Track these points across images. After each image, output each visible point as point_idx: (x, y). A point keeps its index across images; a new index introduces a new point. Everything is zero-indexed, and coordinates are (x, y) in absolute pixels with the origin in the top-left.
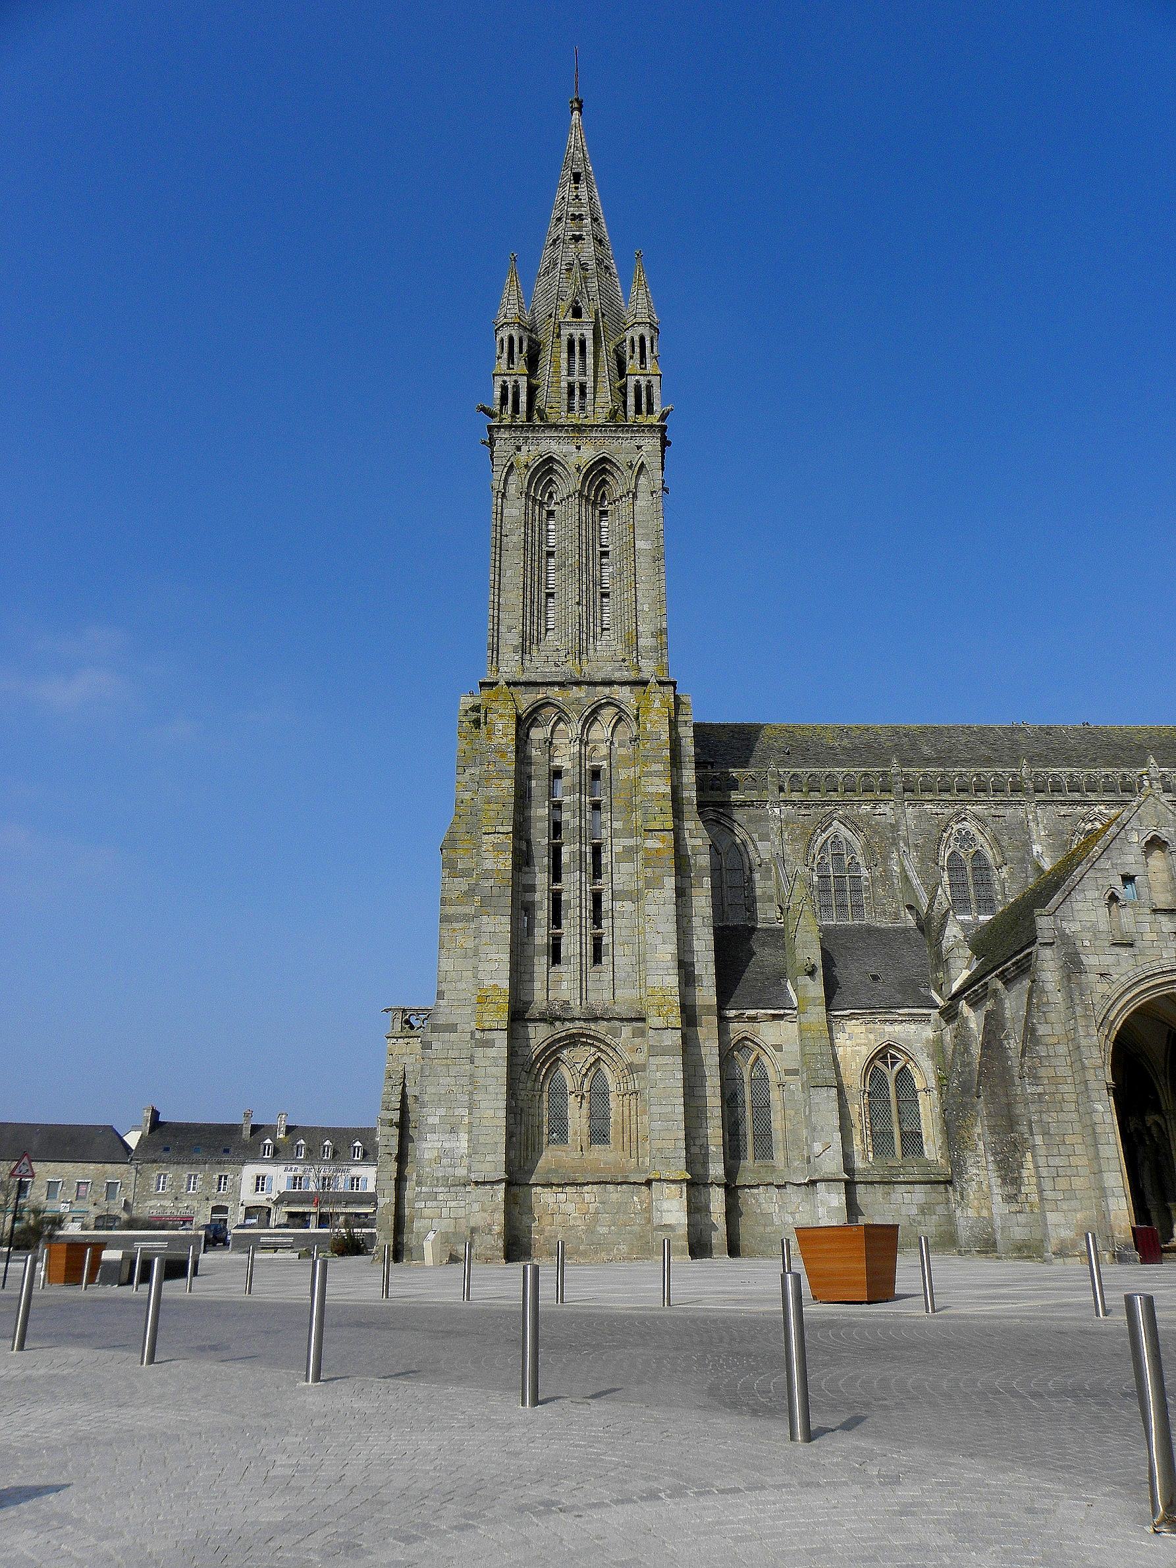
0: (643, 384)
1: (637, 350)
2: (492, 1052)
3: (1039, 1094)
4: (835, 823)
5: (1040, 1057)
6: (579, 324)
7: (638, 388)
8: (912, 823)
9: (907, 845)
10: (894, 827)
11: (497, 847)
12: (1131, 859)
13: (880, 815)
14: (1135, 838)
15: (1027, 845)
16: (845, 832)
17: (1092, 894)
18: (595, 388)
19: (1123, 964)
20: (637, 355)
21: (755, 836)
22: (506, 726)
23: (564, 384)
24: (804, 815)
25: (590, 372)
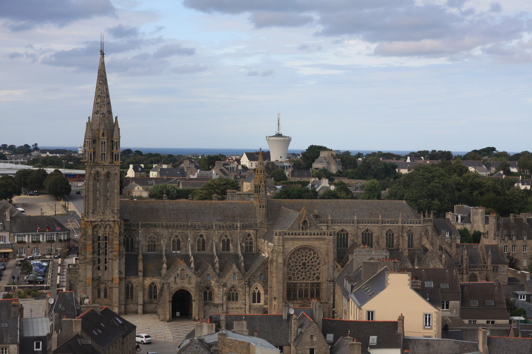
0: (117, 154)
1: (116, 144)
2: (90, 288)
6: (104, 139)
7: (116, 155)
8: (166, 233)
9: (165, 238)
10: (163, 235)
11: (90, 254)
12: (179, 272)
15: (188, 238)
17: (173, 277)
18: (107, 155)
20: (116, 146)
21: (136, 236)
22: (90, 231)
23: (101, 154)
25: (106, 151)
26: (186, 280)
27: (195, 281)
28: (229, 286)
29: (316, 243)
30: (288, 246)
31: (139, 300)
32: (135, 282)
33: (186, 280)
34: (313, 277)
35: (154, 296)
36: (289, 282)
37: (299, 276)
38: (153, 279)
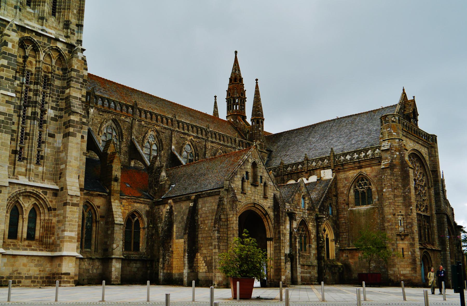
3: (219, 237)
4: (111, 121)
5: (220, 225)
12: (248, 167)
13: (127, 122)
14: (250, 160)
16: (113, 125)
17: (239, 176)
19: (243, 199)
24: (101, 115)
26: (260, 188)
27: (273, 194)
28: (299, 219)
31: (115, 246)
32: (99, 207)
33: (260, 188)
34: (423, 206)
35: (134, 243)
38: (136, 205)
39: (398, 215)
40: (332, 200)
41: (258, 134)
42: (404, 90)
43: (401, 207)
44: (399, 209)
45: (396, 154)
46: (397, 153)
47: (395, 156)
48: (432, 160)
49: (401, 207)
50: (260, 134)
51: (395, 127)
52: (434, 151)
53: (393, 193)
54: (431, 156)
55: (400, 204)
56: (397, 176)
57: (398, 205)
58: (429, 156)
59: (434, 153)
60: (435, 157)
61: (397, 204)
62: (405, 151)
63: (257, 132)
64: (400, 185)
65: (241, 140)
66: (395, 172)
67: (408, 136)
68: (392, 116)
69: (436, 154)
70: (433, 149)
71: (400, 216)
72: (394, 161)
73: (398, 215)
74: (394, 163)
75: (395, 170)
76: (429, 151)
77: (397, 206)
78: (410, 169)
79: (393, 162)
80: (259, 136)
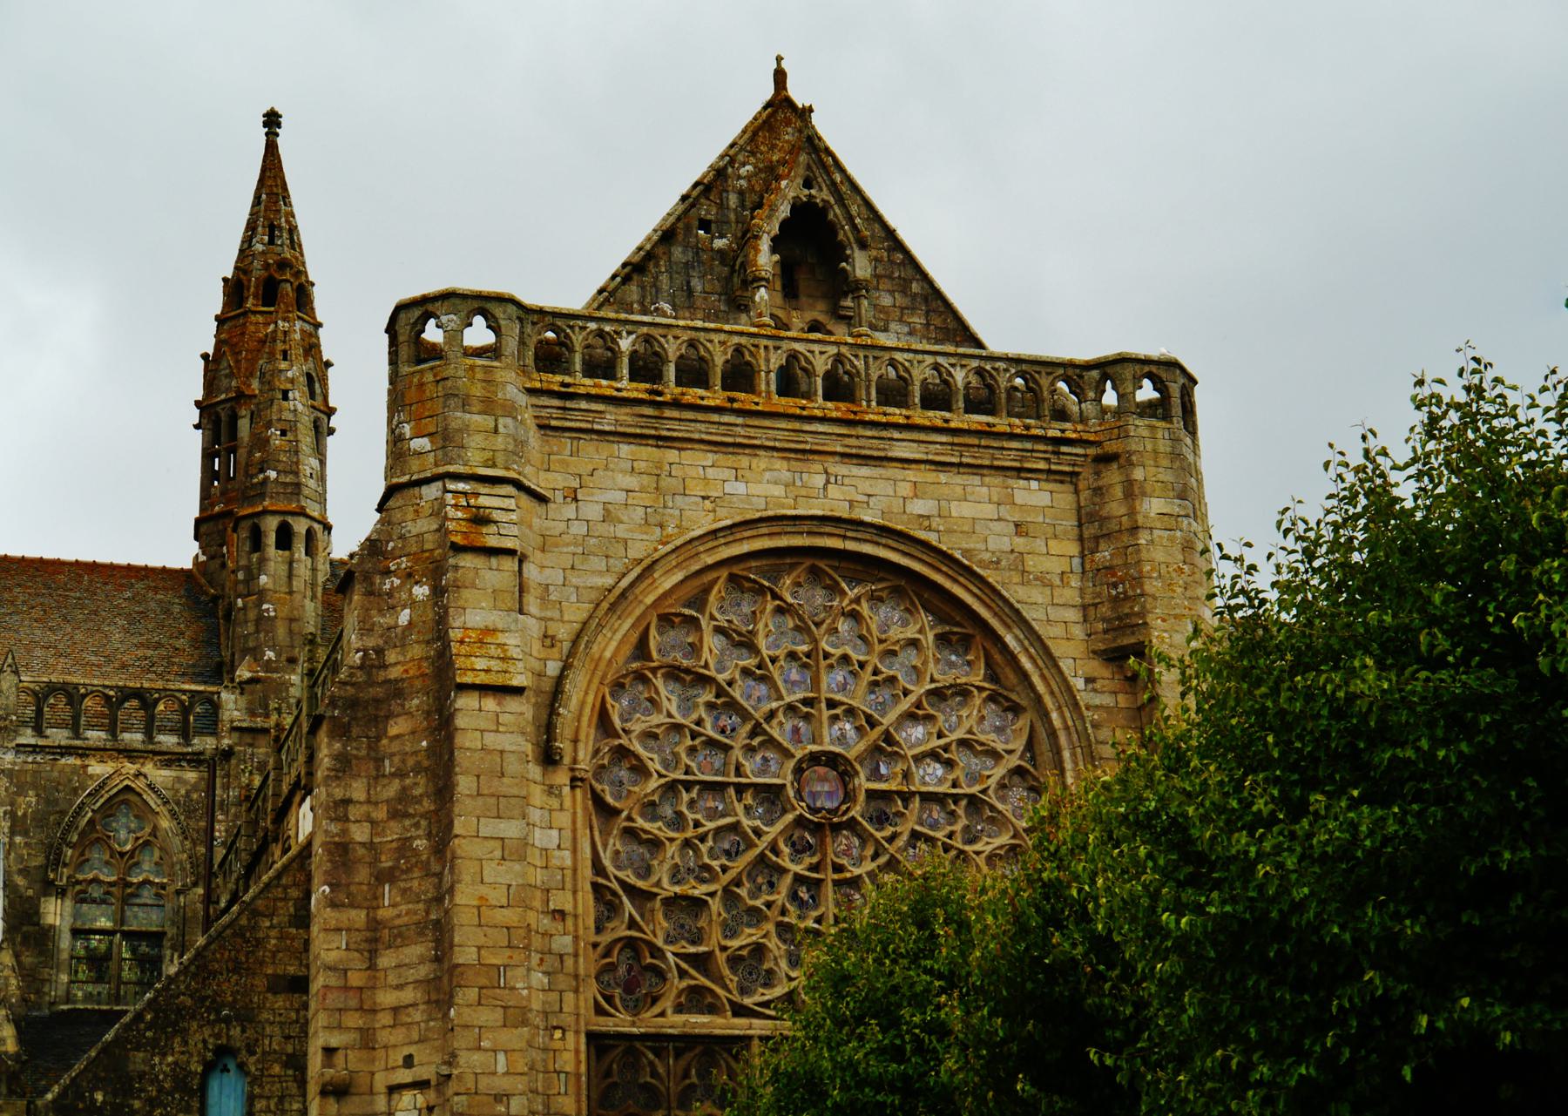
29: (960, 510)
30: (593, 511)
36: (621, 1022)
37: (759, 950)
39: (393, 1089)
40: (246, 1017)
41: (252, 615)
42: (780, 77)
43: (417, 1016)
44: (397, 1036)
45: (413, 604)
46: (421, 592)
47: (404, 617)
48: (1110, 569)
49: (417, 1016)
50: (261, 611)
51: (430, 390)
52: (1118, 492)
53: (359, 917)
54: (1097, 539)
55: (408, 995)
56: (400, 774)
57: (396, 1010)
58: (1081, 539)
59: (1116, 508)
60: (1126, 539)
61: (387, 998)
62: (467, 561)
63: (244, 608)
64: (420, 844)
65: (52, 689)
66: (395, 747)
67: (681, 430)
68: (417, 313)
69: (1132, 513)
70: (1113, 476)
71: (407, 1098)
72: (391, 656)
73: (393, 1089)
74: (394, 673)
75: (393, 730)
76: (1084, 495)
77: (385, 1019)
78: (466, 702)
79: (385, 667)
80: (257, 631)
